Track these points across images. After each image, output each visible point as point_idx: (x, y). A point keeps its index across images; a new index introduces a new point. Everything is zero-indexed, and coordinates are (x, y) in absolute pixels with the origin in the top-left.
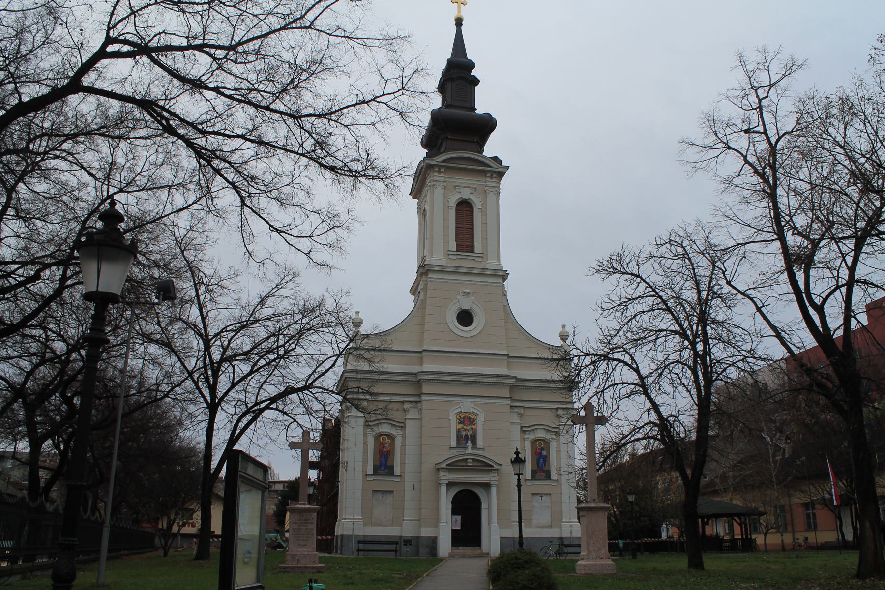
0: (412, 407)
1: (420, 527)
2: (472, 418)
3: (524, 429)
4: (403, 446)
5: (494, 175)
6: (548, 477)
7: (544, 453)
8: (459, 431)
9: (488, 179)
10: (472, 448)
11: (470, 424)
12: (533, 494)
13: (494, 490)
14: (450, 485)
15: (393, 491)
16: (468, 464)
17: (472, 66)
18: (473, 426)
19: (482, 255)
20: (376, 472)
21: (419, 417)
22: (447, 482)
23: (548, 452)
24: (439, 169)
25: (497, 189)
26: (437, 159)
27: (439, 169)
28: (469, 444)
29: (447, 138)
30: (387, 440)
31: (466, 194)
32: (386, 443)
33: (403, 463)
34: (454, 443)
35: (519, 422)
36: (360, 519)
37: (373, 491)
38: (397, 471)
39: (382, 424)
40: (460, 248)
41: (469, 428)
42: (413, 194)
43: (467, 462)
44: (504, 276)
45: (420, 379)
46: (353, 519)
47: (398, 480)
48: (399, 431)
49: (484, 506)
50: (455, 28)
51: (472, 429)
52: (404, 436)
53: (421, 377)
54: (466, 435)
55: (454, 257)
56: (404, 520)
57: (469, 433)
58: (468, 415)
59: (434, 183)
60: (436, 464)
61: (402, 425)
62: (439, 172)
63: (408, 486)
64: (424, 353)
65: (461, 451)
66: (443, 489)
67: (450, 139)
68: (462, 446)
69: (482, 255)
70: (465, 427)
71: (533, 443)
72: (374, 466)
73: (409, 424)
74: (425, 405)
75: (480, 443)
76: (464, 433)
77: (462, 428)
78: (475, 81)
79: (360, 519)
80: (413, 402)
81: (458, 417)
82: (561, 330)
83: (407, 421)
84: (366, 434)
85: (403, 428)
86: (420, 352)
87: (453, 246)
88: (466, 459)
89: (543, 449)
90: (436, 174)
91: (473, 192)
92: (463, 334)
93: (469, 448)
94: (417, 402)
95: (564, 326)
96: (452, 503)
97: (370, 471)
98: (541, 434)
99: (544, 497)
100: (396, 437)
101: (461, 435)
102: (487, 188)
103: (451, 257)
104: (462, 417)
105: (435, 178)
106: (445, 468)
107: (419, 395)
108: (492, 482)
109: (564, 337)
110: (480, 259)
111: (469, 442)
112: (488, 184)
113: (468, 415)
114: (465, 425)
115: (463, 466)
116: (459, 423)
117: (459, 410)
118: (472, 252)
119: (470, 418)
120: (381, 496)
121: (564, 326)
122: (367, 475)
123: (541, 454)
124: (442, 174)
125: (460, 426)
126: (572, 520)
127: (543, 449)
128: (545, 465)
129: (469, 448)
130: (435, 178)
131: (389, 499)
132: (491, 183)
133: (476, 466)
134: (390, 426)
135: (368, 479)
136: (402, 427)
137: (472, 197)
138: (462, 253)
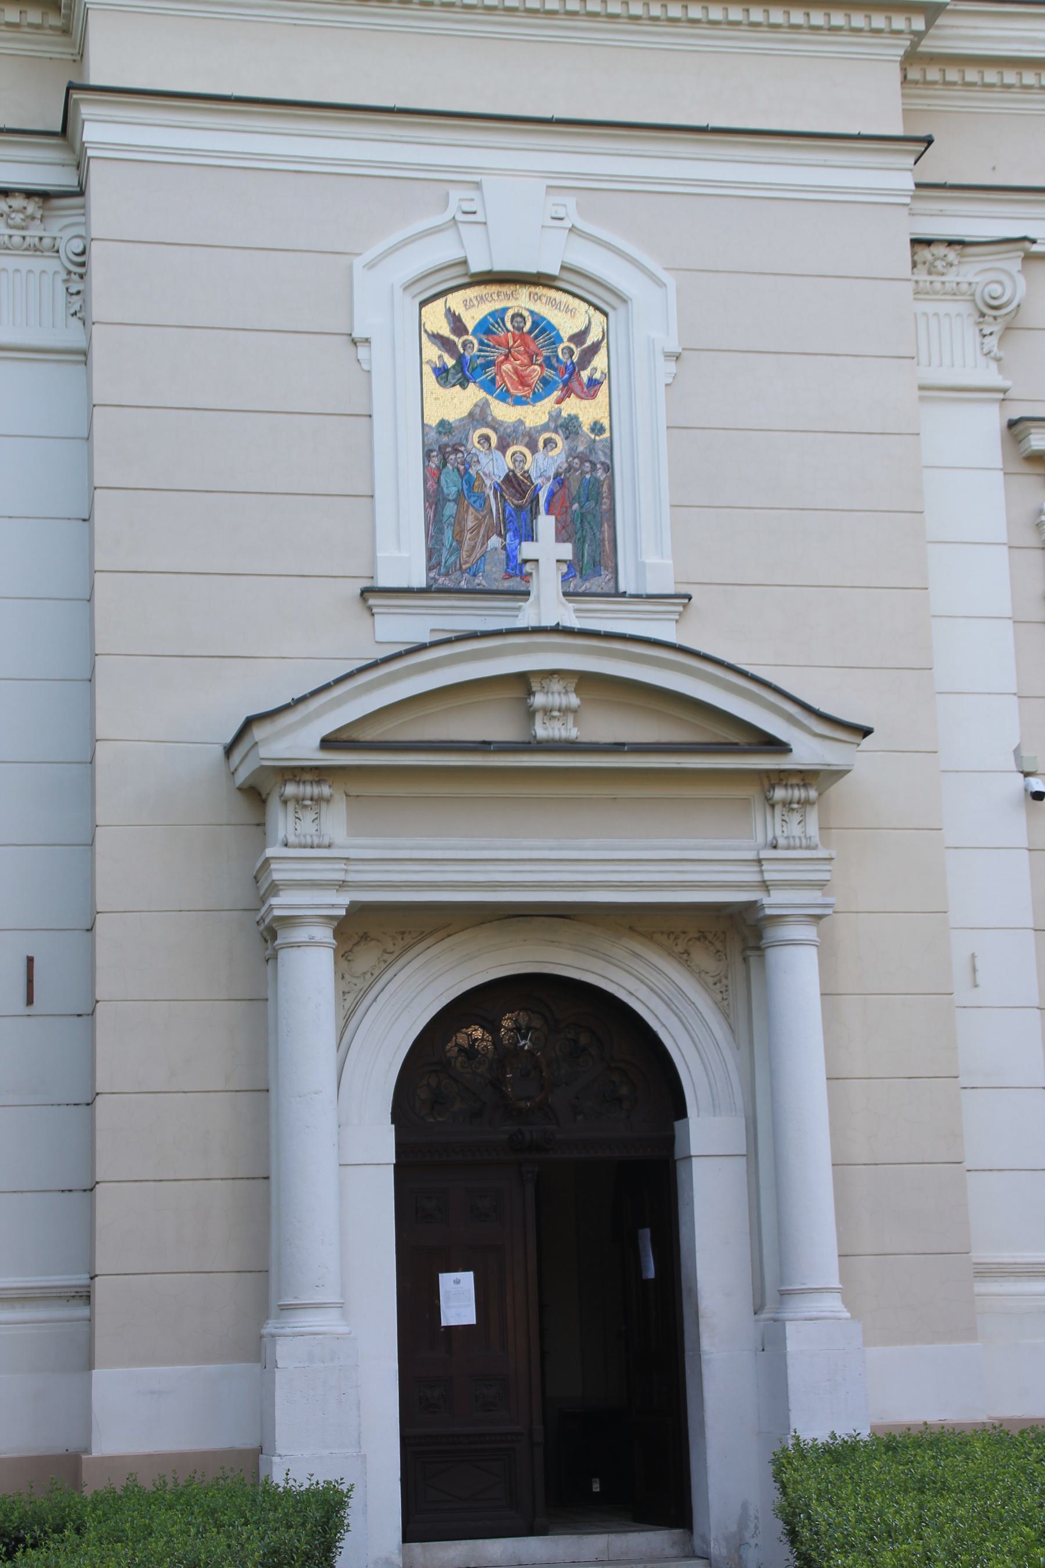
2: (567, 325)
18: (572, 406)
51: (569, 427)
58: (522, 300)
68: (480, 582)
70: (504, 412)
77: (478, 416)
81: (436, 319)
101: (470, 483)
111: (546, 524)
114: (504, 397)
115: (484, 747)
116: (442, 374)
119: (542, 327)
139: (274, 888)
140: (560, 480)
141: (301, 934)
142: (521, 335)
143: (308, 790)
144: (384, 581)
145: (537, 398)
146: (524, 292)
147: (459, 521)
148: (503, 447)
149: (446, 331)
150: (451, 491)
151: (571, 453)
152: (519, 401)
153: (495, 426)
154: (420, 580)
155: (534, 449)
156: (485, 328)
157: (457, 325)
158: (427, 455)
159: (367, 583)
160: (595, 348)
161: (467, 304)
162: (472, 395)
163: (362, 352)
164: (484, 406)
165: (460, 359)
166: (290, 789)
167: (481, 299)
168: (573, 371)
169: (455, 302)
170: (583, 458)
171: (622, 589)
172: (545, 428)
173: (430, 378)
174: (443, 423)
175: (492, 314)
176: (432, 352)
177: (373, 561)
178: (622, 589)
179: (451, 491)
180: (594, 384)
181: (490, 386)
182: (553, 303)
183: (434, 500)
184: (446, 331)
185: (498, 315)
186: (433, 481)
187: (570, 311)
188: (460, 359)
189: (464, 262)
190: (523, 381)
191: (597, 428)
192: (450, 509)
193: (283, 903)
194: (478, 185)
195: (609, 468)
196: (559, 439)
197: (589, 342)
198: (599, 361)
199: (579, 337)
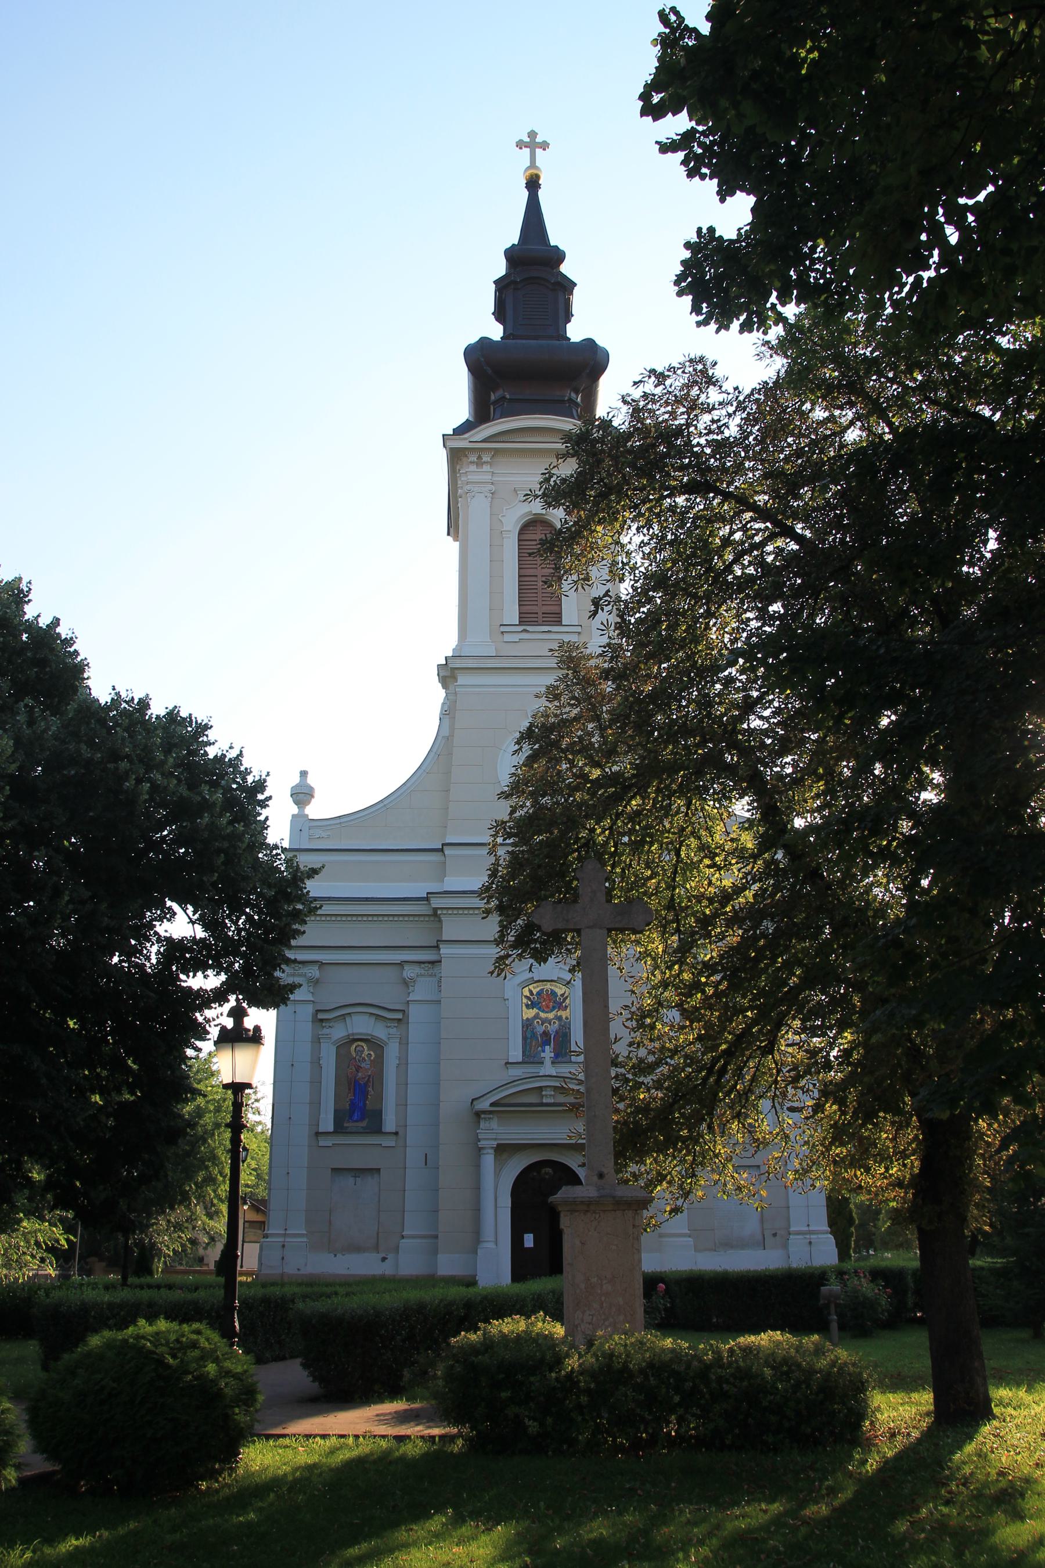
0: (421, 975)
1: (435, 1251)
2: (559, 992)
4: (403, 1063)
8: (527, 1024)
10: (553, 1063)
11: (554, 1008)
14: (503, 1150)
15: (378, 1170)
16: (544, 1101)
17: (558, 256)
19: (579, 629)
20: (339, 1129)
22: (495, 1143)
24: (480, 458)
26: (470, 437)
27: (480, 458)
28: (548, 1053)
29: (504, 397)
30: (366, 1052)
32: (364, 1058)
33: (402, 1105)
34: (516, 1053)
36: (302, 1235)
37: (333, 1169)
38: (390, 1123)
39: (355, 1018)
40: (526, 618)
41: (551, 1016)
42: (452, 530)
43: (542, 1096)
45: (435, 910)
46: (285, 1235)
48: (393, 1031)
50: (526, 193)
51: (560, 1018)
52: (404, 1042)
53: (436, 903)
55: (516, 638)
56: (403, 1237)
57: (552, 1028)
58: (548, 986)
59: (468, 487)
61: (399, 1016)
62: (479, 463)
63: (413, 1156)
64: (448, 851)
65: (531, 1070)
66: (489, 1160)
67: (511, 400)
69: (579, 629)
70: (543, 1015)
72: (335, 1111)
73: (413, 1011)
74: (445, 968)
76: (540, 1029)
77: (537, 1016)
78: (567, 286)
79: (302, 1235)
80: (424, 963)
81: (526, 992)
84: (317, 1040)
85: (402, 1021)
86: (442, 850)
87: (511, 613)
88: (541, 1088)
90: (473, 468)
93: (548, 1062)
94: (433, 963)
97: (327, 1124)
100: (386, 1044)
101: (534, 1034)
103: (507, 638)
105: (472, 477)
106: (491, 1112)
107: (437, 947)
113: (548, 986)
114: (543, 1011)
116: (527, 1006)
118: (559, 622)
119: (553, 993)
120: (351, 1180)
122: (318, 1134)
124: (486, 468)
125: (531, 1013)
129: (548, 1062)
130: (472, 477)
134: (373, 1019)
135: (321, 1143)
136: (399, 1020)
138: (528, 628)
143: (487, 1116)
145: (552, 1011)
147: (531, 1042)
148: (542, 1025)
150: (529, 1036)
151: (560, 1025)
153: (540, 1018)
154: (520, 1060)
155: (550, 1024)
156: (539, 994)
158: (523, 1027)
160: (567, 997)
161: (534, 988)
162: (535, 1010)
163: (507, 1002)
164: (538, 1014)
166: (483, 1116)
167: (538, 986)
168: (561, 1004)
169: (531, 987)
170: (563, 1026)
173: (524, 1008)
174: (527, 1018)
176: (525, 1001)
179: (529, 1036)
180: (566, 1007)
181: (539, 1009)
182: (556, 987)
186: (524, 1033)
187: (560, 988)
188: (532, 1002)
190: (548, 1007)
191: (567, 1018)
192: (529, 1041)
193: (481, 1144)
195: (569, 1029)
198: (567, 1001)
199: (562, 995)
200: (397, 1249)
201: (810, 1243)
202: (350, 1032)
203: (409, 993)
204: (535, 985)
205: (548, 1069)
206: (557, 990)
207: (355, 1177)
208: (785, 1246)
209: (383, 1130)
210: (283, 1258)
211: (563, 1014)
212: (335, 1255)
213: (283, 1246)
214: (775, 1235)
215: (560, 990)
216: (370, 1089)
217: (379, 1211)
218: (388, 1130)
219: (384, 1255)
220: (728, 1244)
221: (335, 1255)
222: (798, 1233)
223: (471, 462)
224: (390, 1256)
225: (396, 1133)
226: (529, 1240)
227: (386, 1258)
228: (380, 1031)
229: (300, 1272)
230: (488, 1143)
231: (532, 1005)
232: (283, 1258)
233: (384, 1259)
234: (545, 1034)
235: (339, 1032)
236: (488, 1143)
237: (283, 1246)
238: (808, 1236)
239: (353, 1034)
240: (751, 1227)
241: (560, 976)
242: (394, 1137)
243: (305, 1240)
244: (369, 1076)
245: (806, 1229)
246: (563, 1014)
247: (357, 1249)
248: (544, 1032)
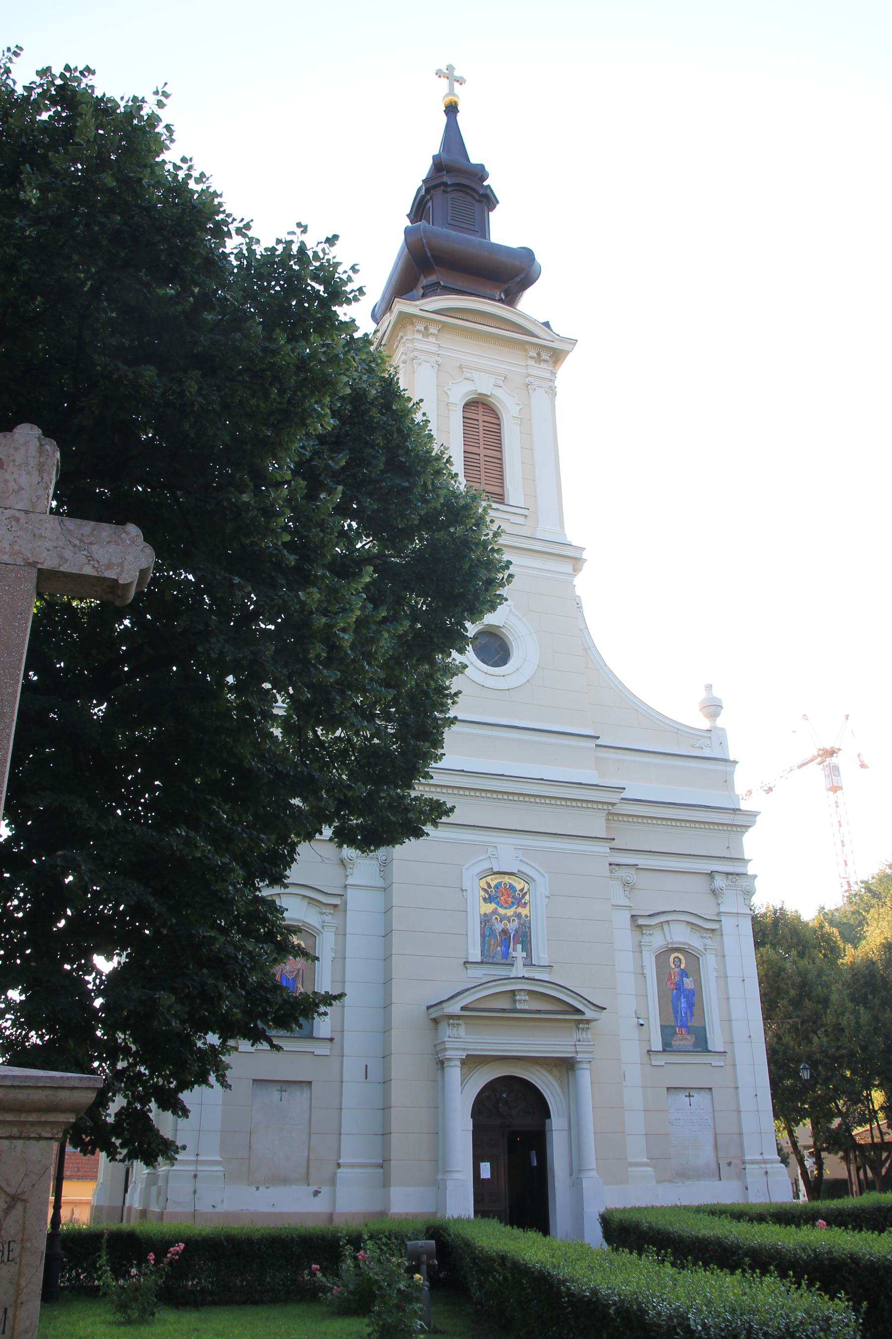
2: (518, 887)
3: (641, 922)
5: (545, 356)
6: (701, 1045)
7: (688, 983)
8: (486, 920)
9: (531, 362)
12: (668, 1089)
13: (585, 1077)
15: (310, 1082)
18: (520, 910)
21: (380, 883)
22: (463, 1054)
23: (698, 982)
25: (551, 384)
26: (422, 305)
31: (484, 386)
34: (475, 954)
35: (626, 902)
37: (254, 1080)
41: (510, 912)
43: (515, 1001)
44: (576, 561)
47: (322, 1049)
48: (328, 918)
49: (557, 1124)
51: (519, 916)
52: (342, 934)
54: (505, 932)
56: (339, 1165)
57: (512, 927)
58: (507, 879)
60: (428, 1008)
61: (336, 901)
63: (352, 1069)
65: (502, 972)
68: (495, 960)
70: (501, 911)
71: (662, 957)
75: (541, 953)
76: (499, 927)
77: (495, 912)
81: (483, 883)
82: (703, 695)
83: (350, 892)
89: (684, 974)
91: (501, 383)
92: (490, 682)
93: (519, 962)
95: (709, 687)
96: (473, 1116)
98: (680, 935)
99: (697, 1097)
101: (492, 931)
102: (530, 379)
104: (493, 884)
108: (579, 1057)
109: (713, 708)
110: (521, 520)
112: (532, 371)
114: (501, 907)
116: (485, 899)
117: (486, 865)
119: (512, 887)
120: (276, 1095)
121: (709, 687)
123: (679, 987)
125: (489, 908)
126: (766, 1157)
127: (684, 974)
128: (692, 1015)
129: (519, 962)
131: (297, 1100)
132: (540, 370)
133: (539, 1012)
134: (305, 902)
136: (335, 906)
137: (498, 393)
139: (446, 1049)
140: (516, 931)
141: (453, 1063)
142: (506, 889)
144: (470, 960)
145: (510, 907)
146: (507, 877)
147: (490, 941)
148: (501, 922)
149: (486, 887)
151: (519, 923)
152: (505, 908)
153: (499, 915)
154: (479, 960)
155: (509, 922)
156: (496, 887)
157: (489, 886)
158: (481, 923)
159: (465, 960)
160: (526, 893)
161: (492, 880)
162: (493, 906)
163: (465, 893)
164: (496, 909)
165: (490, 895)
167: (496, 879)
170: (522, 925)
171: (533, 963)
172: (512, 916)
175: (499, 883)
176: (482, 893)
177: (467, 953)
178: (533, 963)
180: (525, 904)
181: (498, 903)
182: (514, 880)
183: (483, 936)
184: (486, 887)
185: (500, 883)
187: (519, 883)
188: (490, 895)
189: (492, 868)
190: (506, 902)
191: (526, 916)
192: (487, 938)
194: (496, 847)
195: (530, 928)
196: (516, 919)
197: (525, 891)
198: (527, 897)
199: (521, 890)
200: (333, 1182)
201: (766, 1173)
202: (670, 941)
203: (347, 876)
204: (492, 876)
205: (519, 970)
206: (515, 884)
207: (281, 1091)
208: (741, 1174)
209: (315, 1035)
210: (195, 1192)
211: (524, 912)
212: (258, 1188)
213: (195, 1176)
214: (729, 1164)
215: (519, 885)
216: (300, 986)
217: (310, 1134)
218: (322, 1036)
219: (316, 1188)
220: (684, 1174)
221: (258, 1188)
222: (753, 1162)
223: (418, 331)
224: (325, 1190)
225: (331, 1040)
226: (486, 1170)
227: (320, 1192)
228: (694, 941)
229: (217, 1210)
230: (455, 1054)
231: (489, 899)
232: (195, 1192)
233: (316, 1193)
234: (505, 932)
235: (657, 941)
236: (455, 1054)
237: (195, 1176)
238: (763, 1166)
239: (672, 943)
240: (705, 1156)
241: (522, 869)
242: (328, 1044)
243: (220, 1168)
244: (299, 970)
245: (760, 1157)
246: (524, 912)
247: (285, 1181)
248: (503, 930)
